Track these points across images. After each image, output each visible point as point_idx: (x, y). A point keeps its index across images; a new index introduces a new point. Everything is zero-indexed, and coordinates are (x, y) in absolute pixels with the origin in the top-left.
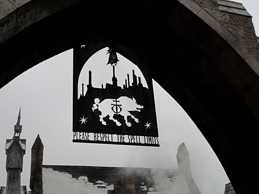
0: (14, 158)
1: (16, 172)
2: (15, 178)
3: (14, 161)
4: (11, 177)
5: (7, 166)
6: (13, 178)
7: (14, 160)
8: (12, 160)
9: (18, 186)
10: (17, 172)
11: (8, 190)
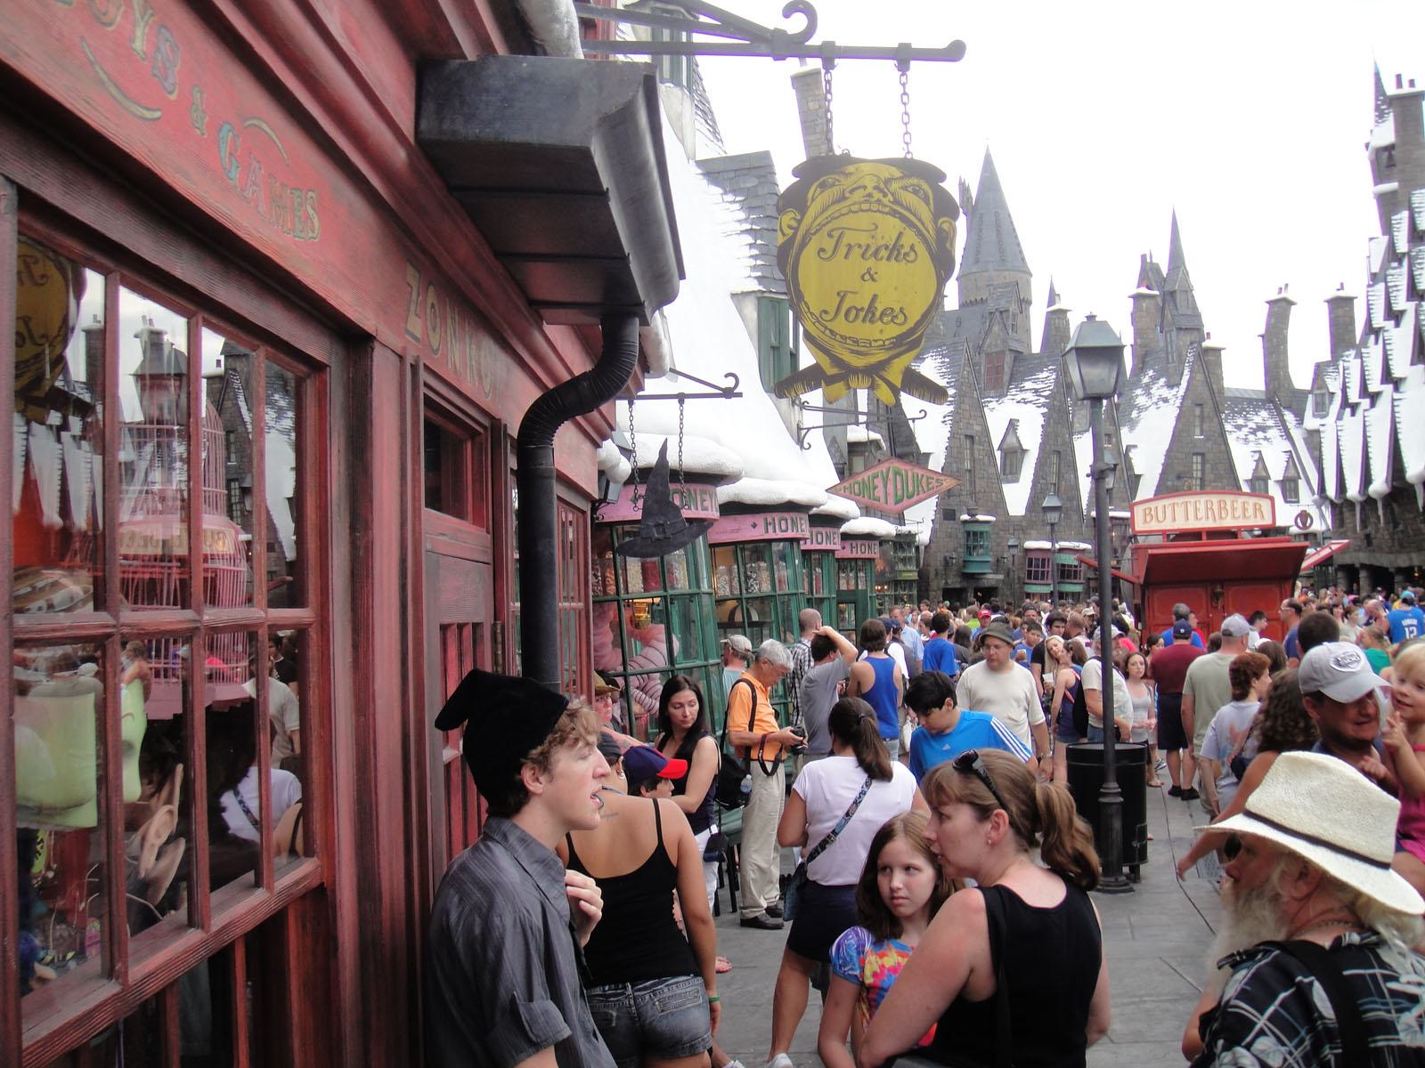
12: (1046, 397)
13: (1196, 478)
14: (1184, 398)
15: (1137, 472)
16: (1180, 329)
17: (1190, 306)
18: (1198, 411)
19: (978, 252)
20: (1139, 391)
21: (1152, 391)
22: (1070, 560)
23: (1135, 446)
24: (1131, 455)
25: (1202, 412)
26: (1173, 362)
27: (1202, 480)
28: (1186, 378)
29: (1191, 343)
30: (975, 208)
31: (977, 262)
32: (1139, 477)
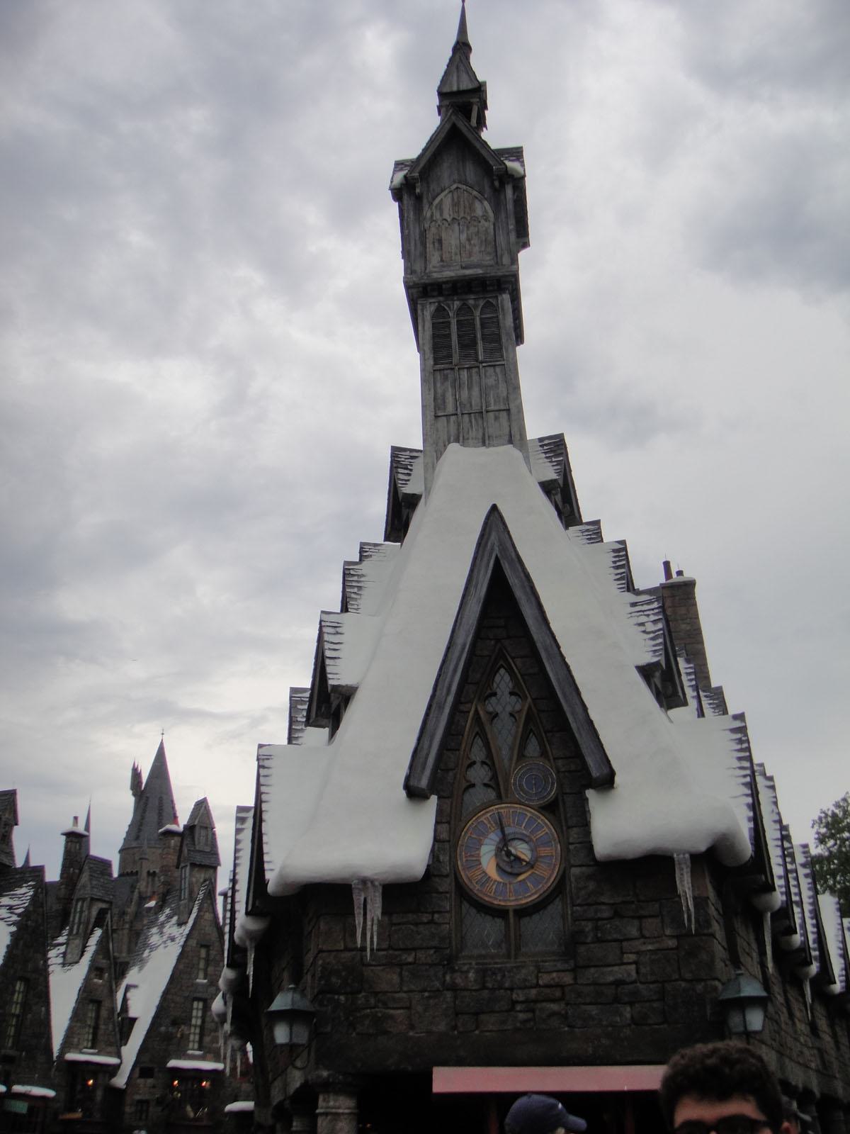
0: (456, 227)
1: (476, 306)
2: (473, 344)
3: (454, 242)
4: (449, 336)
5: (409, 270)
6: (462, 346)
7: (453, 238)
8: (440, 241)
9: (502, 390)
10: (488, 305)
11: (437, 417)
12: (19, 915)
13: (195, 1026)
14: (189, 936)
15: (132, 1014)
16: (193, 865)
17: (209, 843)
18: (203, 953)
19: (140, 830)
20: (154, 930)
21: (165, 930)
22: (21, 1107)
23: (135, 987)
24: (129, 995)
25: (208, 954)
26: (184, 898)
27: (202, 1027)
29: (205, 881)
30: (142, 792)
31: (137, 838)
32: (134, 1020)
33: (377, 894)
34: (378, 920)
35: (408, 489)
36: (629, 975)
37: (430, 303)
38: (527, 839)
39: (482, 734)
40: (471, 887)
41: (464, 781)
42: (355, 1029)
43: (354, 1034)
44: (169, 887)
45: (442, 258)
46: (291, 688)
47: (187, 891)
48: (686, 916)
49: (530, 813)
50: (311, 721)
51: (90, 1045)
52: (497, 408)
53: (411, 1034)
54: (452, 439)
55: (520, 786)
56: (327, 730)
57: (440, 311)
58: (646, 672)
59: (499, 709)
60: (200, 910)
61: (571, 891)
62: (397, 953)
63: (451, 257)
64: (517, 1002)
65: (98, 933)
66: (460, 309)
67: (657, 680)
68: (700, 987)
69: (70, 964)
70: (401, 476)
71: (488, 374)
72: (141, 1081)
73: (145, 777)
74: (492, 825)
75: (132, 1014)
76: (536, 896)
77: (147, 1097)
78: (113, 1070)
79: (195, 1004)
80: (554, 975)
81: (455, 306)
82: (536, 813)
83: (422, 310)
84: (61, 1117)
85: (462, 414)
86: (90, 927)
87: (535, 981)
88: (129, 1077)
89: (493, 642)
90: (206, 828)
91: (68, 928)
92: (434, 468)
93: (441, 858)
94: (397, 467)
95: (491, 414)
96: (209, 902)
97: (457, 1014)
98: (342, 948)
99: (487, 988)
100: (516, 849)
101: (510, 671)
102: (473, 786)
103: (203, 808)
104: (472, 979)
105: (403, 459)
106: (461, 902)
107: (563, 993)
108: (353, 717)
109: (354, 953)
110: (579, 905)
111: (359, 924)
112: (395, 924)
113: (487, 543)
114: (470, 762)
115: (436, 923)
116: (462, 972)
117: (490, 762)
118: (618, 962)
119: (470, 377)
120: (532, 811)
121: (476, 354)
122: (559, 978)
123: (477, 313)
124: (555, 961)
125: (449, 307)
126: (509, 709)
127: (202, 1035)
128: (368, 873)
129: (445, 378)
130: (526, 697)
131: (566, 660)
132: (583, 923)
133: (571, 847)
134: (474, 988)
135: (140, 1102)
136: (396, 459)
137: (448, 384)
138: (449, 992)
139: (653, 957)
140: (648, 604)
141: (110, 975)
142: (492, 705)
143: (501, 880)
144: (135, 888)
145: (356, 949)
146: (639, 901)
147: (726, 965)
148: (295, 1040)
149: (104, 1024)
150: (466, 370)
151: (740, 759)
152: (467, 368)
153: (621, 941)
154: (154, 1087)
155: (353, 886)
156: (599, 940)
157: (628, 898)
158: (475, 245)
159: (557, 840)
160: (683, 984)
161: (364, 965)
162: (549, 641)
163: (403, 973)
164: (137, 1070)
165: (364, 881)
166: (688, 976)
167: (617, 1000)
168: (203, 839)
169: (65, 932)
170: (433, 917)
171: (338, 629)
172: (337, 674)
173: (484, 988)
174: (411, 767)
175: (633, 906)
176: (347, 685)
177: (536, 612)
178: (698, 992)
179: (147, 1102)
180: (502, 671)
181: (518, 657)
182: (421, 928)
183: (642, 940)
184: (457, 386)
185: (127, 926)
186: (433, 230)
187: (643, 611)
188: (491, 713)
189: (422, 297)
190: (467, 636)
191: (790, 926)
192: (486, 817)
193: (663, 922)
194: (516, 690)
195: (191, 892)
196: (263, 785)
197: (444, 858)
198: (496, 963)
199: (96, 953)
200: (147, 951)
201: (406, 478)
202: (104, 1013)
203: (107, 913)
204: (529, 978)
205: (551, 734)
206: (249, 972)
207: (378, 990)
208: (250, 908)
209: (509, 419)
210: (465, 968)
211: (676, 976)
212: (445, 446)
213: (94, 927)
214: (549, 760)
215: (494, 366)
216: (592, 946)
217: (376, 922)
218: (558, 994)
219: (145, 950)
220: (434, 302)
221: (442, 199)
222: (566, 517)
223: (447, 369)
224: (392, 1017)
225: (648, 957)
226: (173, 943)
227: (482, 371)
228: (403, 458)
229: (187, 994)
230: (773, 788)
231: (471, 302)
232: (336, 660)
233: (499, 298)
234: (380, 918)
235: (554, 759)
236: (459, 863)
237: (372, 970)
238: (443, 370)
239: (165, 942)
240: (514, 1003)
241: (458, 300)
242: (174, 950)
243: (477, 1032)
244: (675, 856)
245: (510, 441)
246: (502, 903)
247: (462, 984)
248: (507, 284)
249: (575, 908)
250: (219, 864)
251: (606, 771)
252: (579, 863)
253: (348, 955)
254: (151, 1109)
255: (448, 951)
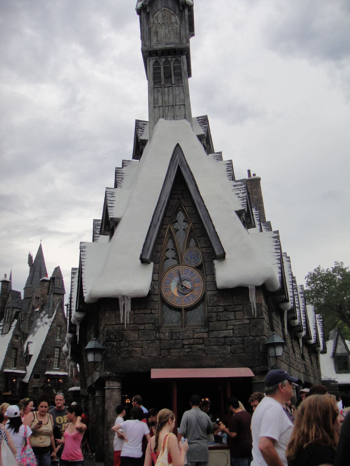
0: (164, 26)
1: (171, 61)
2: (170, 76)
3: (163, 33)
4: (160, 73)
5: (143, 45)
6: (166, 78)
7: (162, 31)
8: (157, 33)
9: (182, 96)
11: (154, 107)
13: (56, 358)
14: (53, 322)
15: (30, 353)
16: (54, 293)
17: (61, 284)
18: (59, 328)
19: (32, 280)
20: (39, 320)
21: (43, 320)
23: (31, 342)
24: (29, 346)
25: (61, 329)
27: (59, 358)
28: (55, 314)
29: (59, 300)
31: (31, 283)
33: (129, 302)
34: (129, 312)
35: (142, 137)
36: (230, 334)
37: (152, 59)
38: (190, 280)
39: (172, 237)
40: (167, 299)
41: (164, 257)
42: (120, 356)
43: (120, 358)
44: (45, 303)
45: (157, 40)
46: (94, 220)
47: (52, 304)
48: (253, 311)
49: (191, 269)
50: (102, 233)
51: (13, 366)
52: (180, 104)
53: (143, 357)
54: (161, 117)
55: (187, 258)
56: (108, 236)
57: (156, 63)
58: (239, 213)
59: (179, 227)
60: (57, 312)
61: (207, 301)
62: (137, 325)
63: (161, 39)
64: (185, 345)
65: (16, 321)
66: (165, 62)
67: (243, 216)
68: (258, 339)
69: (5, 334)
70: (139, 132)
71: (176, 90)
72: (35, 380)
73: (34, 258)
74: (175, 274)
75: (30, 353)
76: (193, 303)
77: (37, 386)
78: (24, 375)
79: (56, 349)
80: (200, 334)
81: (163, 61)
82: (194, 270)
83: (149, 62)
84: (3, 394)
85: (165, 106)
86: (13, 318)
87: (192, 336)
88: (30, 378)
89: (177, 200)
90: (60, 278)
91: (3, 319)
92: (153, 128)
93: (155, 287)
94: (138, 128)
95: (177, 106)
96: (61, 308)
97: (161, 349)
98: (115, 323)
99: (174, 339)
100: (185, 284)
101: (183, 212)
102: (168, 258)
103: (58, 270)
104: (167, 336)
105: (140, 125)
106: (163, 305)
107: (204, 341)
108: (119, 231)
109: (120, 325)
110: (210, 306)
111: (122, 313)
112: (136, 314)
113: (174, 159)
114: (167, 249)
115: (152, 313)
116: (163, 333)
117: (175, 249)
118: (226, 329)
119: (169, 91)
120: (192, 269)
121: (171, 81)
122: (202, 335)
123: (172, 64)
124: (200, 328)
125: (160, 61)
126: (183, 227)
127: (59, 361)
128: (125, 293)
129: (158, 91)
130: (190, 223)
131: (206, 207)
132: (212, 313)
133: (208, 283)
134: (168, 339)
135: (34, 388)
136: (137, 125)
137: (160, 94)
138: (158, 341)
139: (240, 327)
140: (240, 186)
141: (21, 338)
142: (176, 226)
143: (179, 296)
144: (31, 304)
145: (120, 324)
146: (234, 305)
147: (269, 331)
148: (96, 360)
149: (19, 358)
150: (167, 88)
151: (276, 249)
152: (168, 87)
153: (227, 321)
154: (40, 382)
155: (119, 299)
156: (218, 320)
157: (230, 304)
158: (172, 35)
159: (202, 281)
160: (251, 338)
161: (124, 330)
162: (200, 200)
163: (139, 333)
164: (33, 375)
165: (124, 297)
166: (254, 334)
167: (225, 344)
168: (58, 283)
169: (2, 321)
170: (151, 311)
171: (113, 195)
172: (112, 213)
173: (172, 339)
174: (143, 251)
175: (232, 307)
176: (116, 218)
177: (194, 188)
178: (257, 341)
179: (37, 388)
180: (180, 212)
181: (186, 206)
182: (147, 315)
183: (235, 320)
184: (163, 94)
185: (28, 319)
186: (154, 28)
187: (239, 189)
188: (176, 229)
189: (149, 57)
190: (166, 198)
191: (295, 317)
192: (173, 271)
193: (244, 313)
194: (186, 220)
195: (53, 305)
196: (82, 259)
197: (156, 287)
198: (177, 329)
199: (15, 329)
200: (36, 328)
201: (142, 133)
202: (19, 353)
203: (19, 313)
204: (190, 335)
205: (199, 238)
206: (77, 334)
207: (129, 340)
208: (77, 309)
209: (185, 109)
210: (165, 331)
211: (249, 334)
212: (158, 120)
213: (14, 319)
214: (199, 249)
215: (179, 86)
216: (215, 322)
217: (128, 313)
218: (201, 341)
219: (35, 328)
220: (154, 59)
221: (158, 15)
222: (207, 150)
223: (159, 87)
224: (135, 351)
225: (237, 327)
226: (47, 325)
227: (174, 88)
228: (140, 124)
229: (52, 345)
230: (289, 261)
231: (170, 59)
232: (112, 208)
233: (182, 57)
234: (130, 312)
235: (201, 248)
236: (162, 289)
237: (127, 333)
238: (157, 87)
239: (43, 325)
240: (184, 345)
241: (164, 58)
242: (47, 328)
243: (169, 356)
244: (249, 287)
245: (185, 118)
246: (180, 306)
247: (163, 338)
248: (185, 52)
249: (209, 307)
250: (65, 293)
251: (222, 253)
252: (211, 290)
253: (117, 326)
254: (39, 391)
255: (157, 325)
